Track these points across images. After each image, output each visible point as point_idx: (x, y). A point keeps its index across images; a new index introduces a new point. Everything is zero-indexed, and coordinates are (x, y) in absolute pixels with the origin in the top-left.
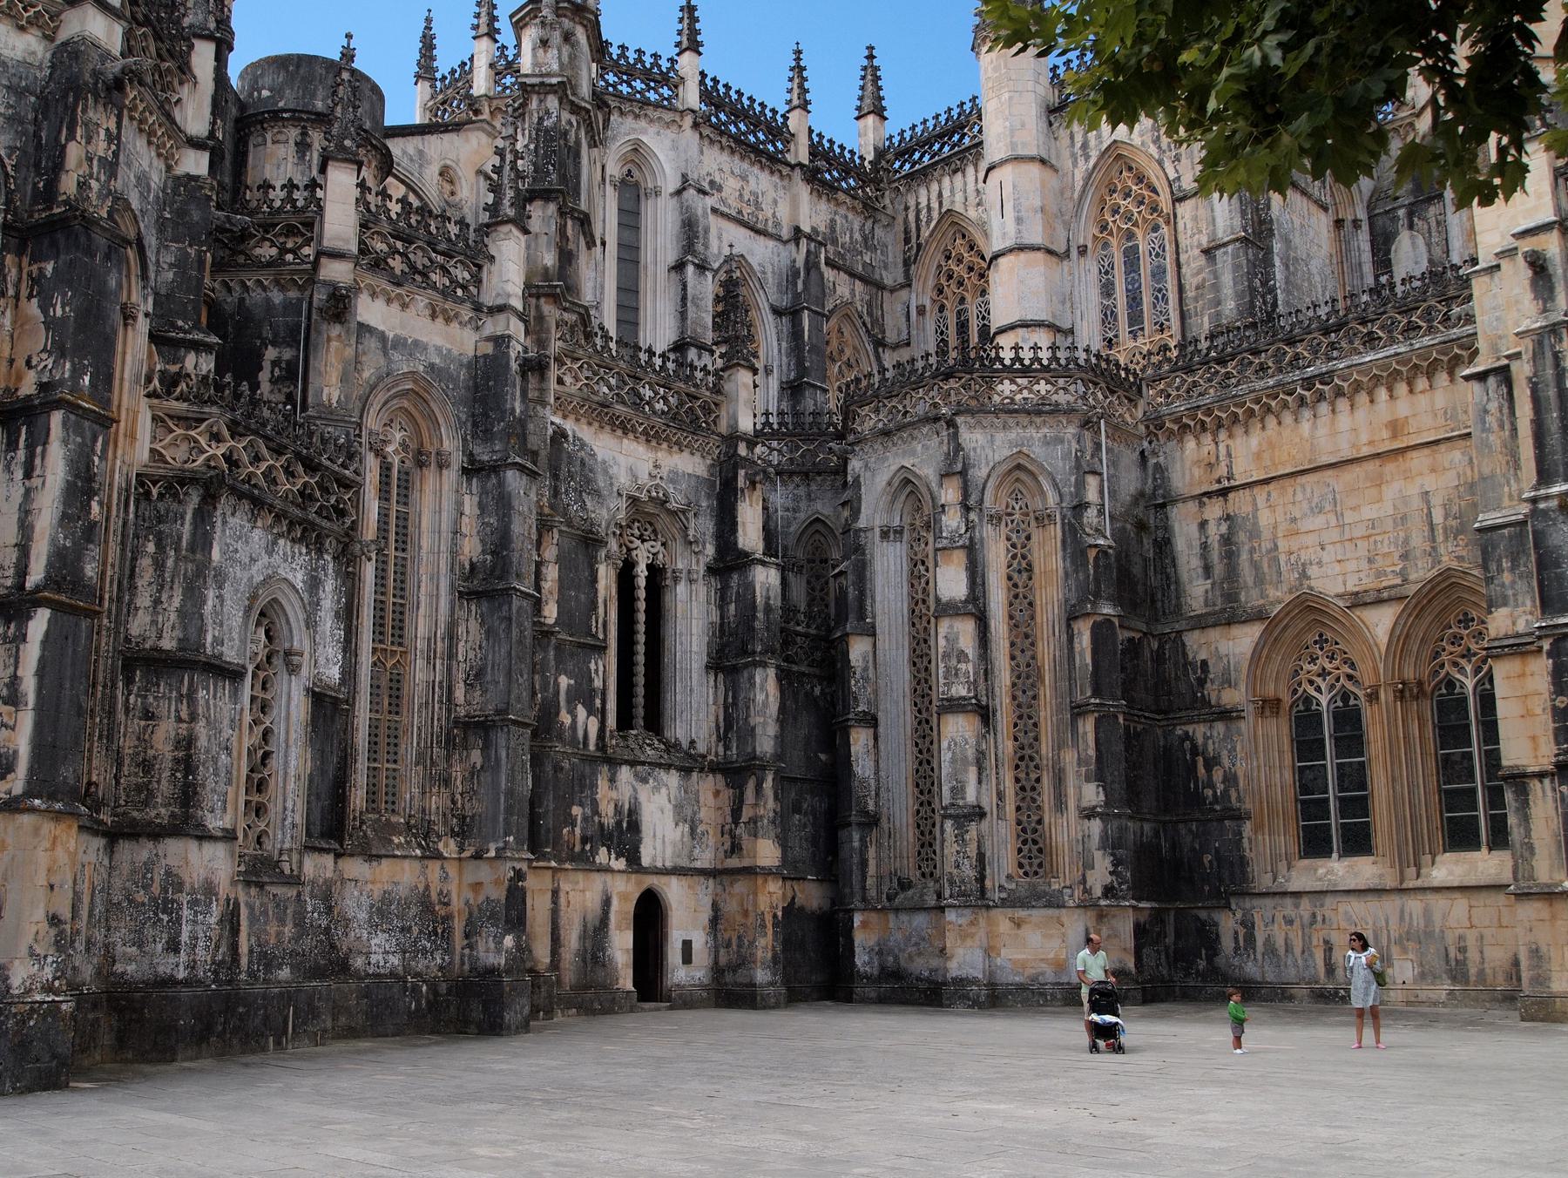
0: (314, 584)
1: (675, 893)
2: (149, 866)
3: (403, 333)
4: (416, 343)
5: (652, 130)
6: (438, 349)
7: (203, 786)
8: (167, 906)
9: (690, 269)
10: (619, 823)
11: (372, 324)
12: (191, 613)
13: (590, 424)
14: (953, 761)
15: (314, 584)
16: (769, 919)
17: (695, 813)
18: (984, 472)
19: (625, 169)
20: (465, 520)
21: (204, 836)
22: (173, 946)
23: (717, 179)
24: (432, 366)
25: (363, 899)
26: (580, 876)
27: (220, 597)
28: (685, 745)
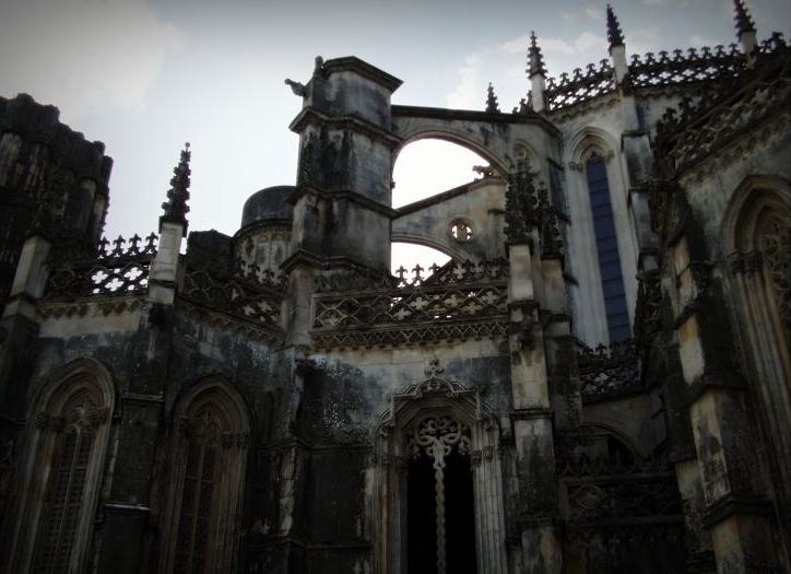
5: (598, 116)
6: (108, 336)
9: (635, 197)
13: (355, 349)
18: (719, 218)
19: (588, 154)
24: (100, 349)
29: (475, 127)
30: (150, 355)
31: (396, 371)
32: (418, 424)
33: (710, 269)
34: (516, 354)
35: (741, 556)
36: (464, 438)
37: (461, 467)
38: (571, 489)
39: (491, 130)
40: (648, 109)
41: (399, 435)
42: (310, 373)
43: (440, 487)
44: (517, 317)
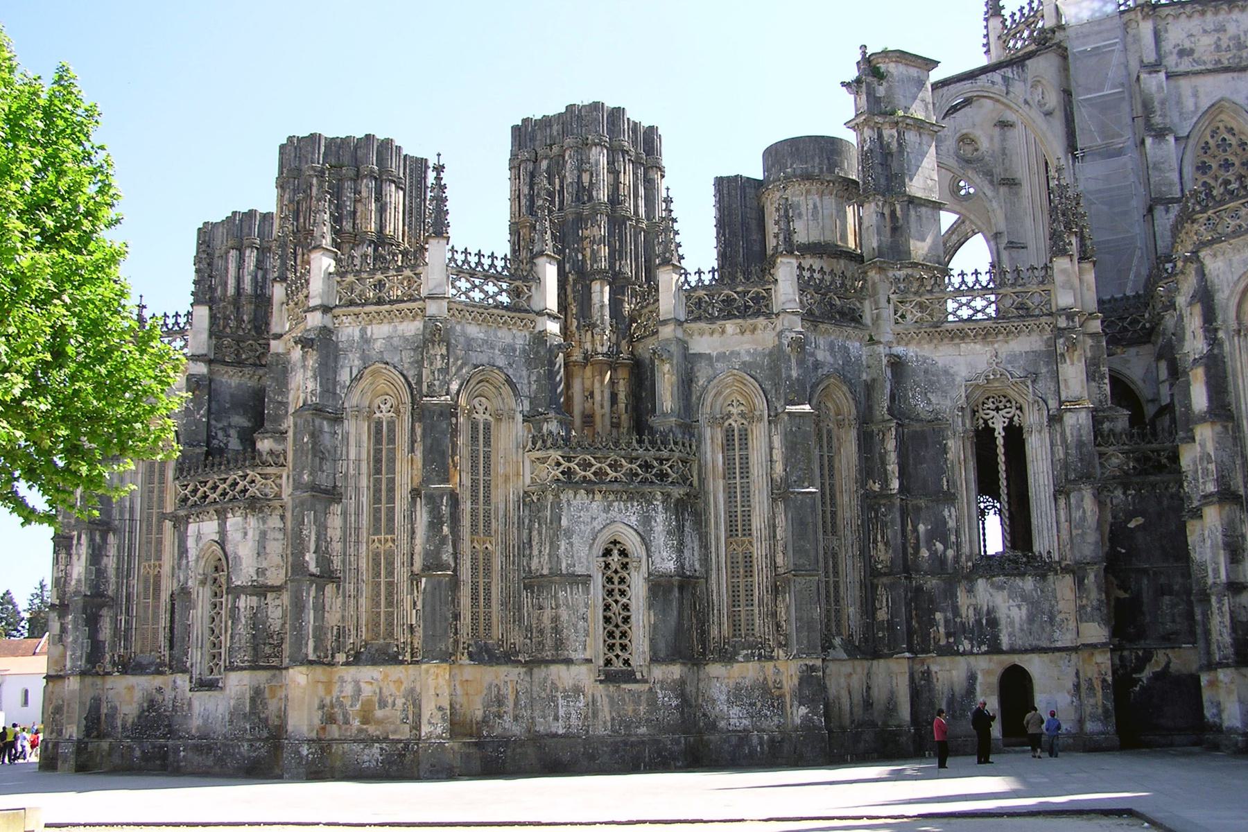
0: (646, 520)
1: (1035, 666)
2: (545, 680)
3: (721, 350)
4: (732, 353)
6: (748, 352)
7: (568, 639)
8: (553, 699)
9: (1149, 141)
10: (979, 622)
11: (702, 351)
12: (554, 556)
14: (1212, 546)
15: (646, 520)
16: (1097, 684)
17: (1053, 607)
18: (1227, 293)
20: (775, 451)
21: (568, 662)
22: (556, 719)
23: (1187, 45)
24: (744, 363)
25: (723, 687)
26: (946, 659)
27: (571, 544)
28: (1045, 555)
29: (997, 76)
30: (794, 374)
31: (965, 362)
32: (981, 400)
33: (1216, 330)
34: (1062, 355)
35: (1220, 529)
36: (1018, 412)
37: (1015, 435)
38: (1101, 455)
39: (1011, 75)
40: (1166, 31)
41: (968, 411)
42: (897, 364)
43: (1001, 450)
44: (1062, 323)
